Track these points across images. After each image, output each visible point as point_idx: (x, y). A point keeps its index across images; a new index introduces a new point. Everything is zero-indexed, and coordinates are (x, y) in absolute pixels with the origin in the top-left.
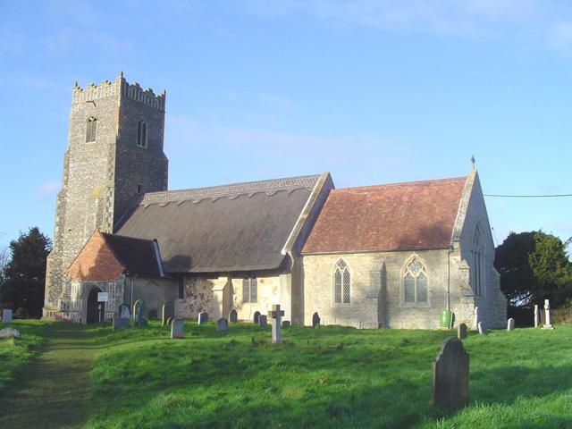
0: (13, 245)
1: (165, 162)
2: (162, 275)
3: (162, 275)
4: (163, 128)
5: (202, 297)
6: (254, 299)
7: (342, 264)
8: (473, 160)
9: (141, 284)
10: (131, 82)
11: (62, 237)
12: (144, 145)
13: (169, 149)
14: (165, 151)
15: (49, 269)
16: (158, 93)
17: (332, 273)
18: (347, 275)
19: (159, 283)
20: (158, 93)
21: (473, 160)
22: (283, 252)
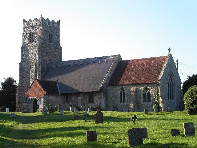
0: (2, 84)
1: (61, 48)
2: (60, 94)
3: (60, 94)
4: (59, 35)
5: (75, 101)
6: (93, 102)
7: (122, 89)
8: (170, 50)
9: (52, 98)
10: (45, 18)
11: (22, 80)
12: (52, 43)
13: (61, 44)
14: (61, 44)
15: (17, 93)
16: (56, 21)
17: (119, 92)
18: (124, 93)
19: (59, 97)
20: (56, 21)
21: (170, 50)
22: (102, 85)
